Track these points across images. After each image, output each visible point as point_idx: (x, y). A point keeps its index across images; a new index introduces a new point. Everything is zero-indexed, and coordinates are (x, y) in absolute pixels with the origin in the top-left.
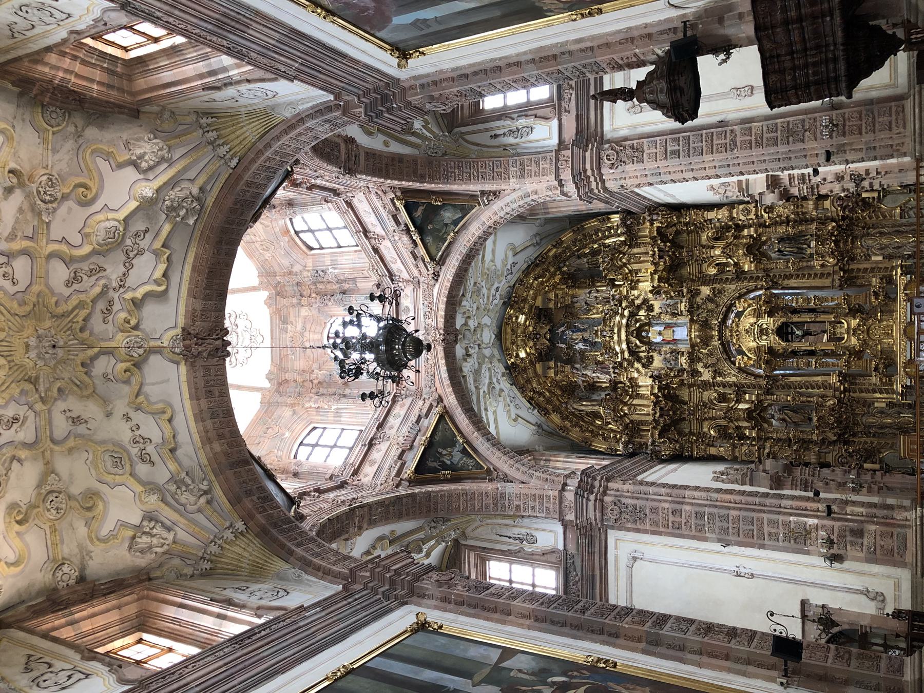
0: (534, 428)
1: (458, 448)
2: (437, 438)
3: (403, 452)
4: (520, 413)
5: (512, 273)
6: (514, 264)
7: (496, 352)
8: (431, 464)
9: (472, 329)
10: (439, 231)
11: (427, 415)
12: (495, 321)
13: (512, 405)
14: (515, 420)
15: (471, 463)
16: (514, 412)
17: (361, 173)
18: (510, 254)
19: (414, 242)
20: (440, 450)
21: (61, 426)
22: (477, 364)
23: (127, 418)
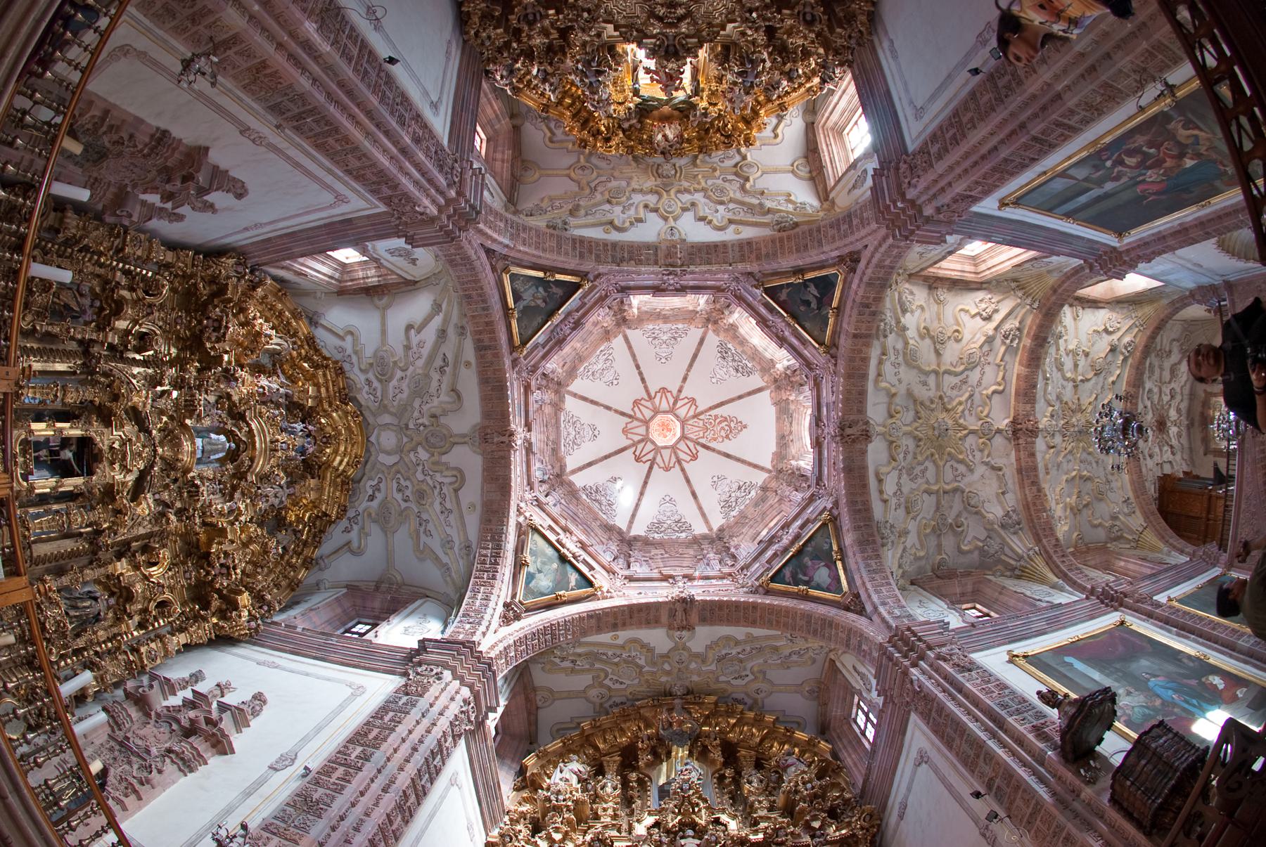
0: (323, 322)
1: (522, 304)
2: (539, 320)
3: (577, 311)
4: (338, 342)
5: (349, 519)
6: (347, 530)
7: (371, 420)
8: (558, 292)
9: (420, 449)
10: (544, 563)
11: (536, 346)
12: (372, 458)
13: (349, 351)
14: (351, 333)
15: (518, 285)
16: (348, 344)
17: (665, 603)
18: (355, 545)
19: (563, 546)
20: (543, 305)
21: (932, 380)
22: (417, 403)
23: (900, 381)
